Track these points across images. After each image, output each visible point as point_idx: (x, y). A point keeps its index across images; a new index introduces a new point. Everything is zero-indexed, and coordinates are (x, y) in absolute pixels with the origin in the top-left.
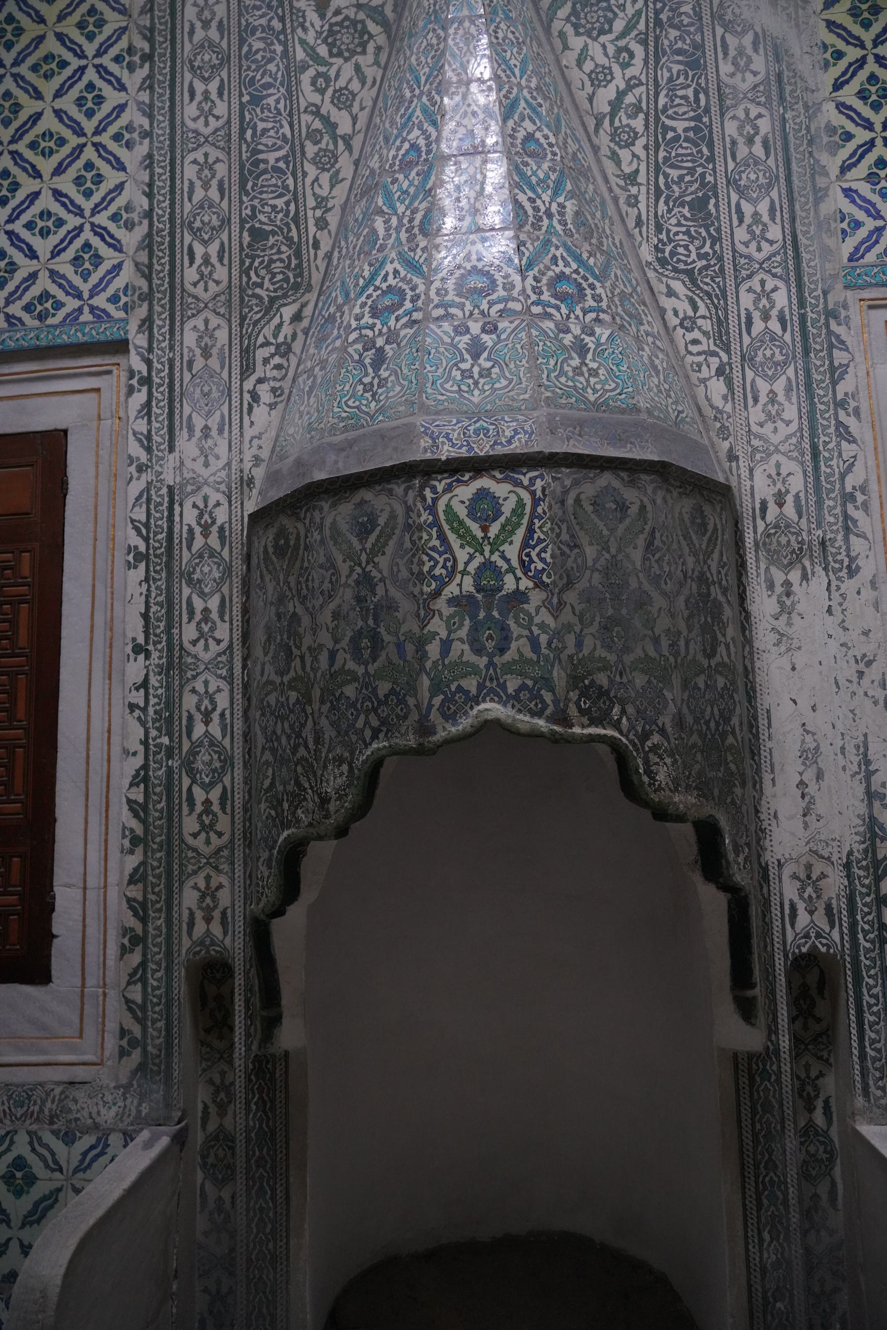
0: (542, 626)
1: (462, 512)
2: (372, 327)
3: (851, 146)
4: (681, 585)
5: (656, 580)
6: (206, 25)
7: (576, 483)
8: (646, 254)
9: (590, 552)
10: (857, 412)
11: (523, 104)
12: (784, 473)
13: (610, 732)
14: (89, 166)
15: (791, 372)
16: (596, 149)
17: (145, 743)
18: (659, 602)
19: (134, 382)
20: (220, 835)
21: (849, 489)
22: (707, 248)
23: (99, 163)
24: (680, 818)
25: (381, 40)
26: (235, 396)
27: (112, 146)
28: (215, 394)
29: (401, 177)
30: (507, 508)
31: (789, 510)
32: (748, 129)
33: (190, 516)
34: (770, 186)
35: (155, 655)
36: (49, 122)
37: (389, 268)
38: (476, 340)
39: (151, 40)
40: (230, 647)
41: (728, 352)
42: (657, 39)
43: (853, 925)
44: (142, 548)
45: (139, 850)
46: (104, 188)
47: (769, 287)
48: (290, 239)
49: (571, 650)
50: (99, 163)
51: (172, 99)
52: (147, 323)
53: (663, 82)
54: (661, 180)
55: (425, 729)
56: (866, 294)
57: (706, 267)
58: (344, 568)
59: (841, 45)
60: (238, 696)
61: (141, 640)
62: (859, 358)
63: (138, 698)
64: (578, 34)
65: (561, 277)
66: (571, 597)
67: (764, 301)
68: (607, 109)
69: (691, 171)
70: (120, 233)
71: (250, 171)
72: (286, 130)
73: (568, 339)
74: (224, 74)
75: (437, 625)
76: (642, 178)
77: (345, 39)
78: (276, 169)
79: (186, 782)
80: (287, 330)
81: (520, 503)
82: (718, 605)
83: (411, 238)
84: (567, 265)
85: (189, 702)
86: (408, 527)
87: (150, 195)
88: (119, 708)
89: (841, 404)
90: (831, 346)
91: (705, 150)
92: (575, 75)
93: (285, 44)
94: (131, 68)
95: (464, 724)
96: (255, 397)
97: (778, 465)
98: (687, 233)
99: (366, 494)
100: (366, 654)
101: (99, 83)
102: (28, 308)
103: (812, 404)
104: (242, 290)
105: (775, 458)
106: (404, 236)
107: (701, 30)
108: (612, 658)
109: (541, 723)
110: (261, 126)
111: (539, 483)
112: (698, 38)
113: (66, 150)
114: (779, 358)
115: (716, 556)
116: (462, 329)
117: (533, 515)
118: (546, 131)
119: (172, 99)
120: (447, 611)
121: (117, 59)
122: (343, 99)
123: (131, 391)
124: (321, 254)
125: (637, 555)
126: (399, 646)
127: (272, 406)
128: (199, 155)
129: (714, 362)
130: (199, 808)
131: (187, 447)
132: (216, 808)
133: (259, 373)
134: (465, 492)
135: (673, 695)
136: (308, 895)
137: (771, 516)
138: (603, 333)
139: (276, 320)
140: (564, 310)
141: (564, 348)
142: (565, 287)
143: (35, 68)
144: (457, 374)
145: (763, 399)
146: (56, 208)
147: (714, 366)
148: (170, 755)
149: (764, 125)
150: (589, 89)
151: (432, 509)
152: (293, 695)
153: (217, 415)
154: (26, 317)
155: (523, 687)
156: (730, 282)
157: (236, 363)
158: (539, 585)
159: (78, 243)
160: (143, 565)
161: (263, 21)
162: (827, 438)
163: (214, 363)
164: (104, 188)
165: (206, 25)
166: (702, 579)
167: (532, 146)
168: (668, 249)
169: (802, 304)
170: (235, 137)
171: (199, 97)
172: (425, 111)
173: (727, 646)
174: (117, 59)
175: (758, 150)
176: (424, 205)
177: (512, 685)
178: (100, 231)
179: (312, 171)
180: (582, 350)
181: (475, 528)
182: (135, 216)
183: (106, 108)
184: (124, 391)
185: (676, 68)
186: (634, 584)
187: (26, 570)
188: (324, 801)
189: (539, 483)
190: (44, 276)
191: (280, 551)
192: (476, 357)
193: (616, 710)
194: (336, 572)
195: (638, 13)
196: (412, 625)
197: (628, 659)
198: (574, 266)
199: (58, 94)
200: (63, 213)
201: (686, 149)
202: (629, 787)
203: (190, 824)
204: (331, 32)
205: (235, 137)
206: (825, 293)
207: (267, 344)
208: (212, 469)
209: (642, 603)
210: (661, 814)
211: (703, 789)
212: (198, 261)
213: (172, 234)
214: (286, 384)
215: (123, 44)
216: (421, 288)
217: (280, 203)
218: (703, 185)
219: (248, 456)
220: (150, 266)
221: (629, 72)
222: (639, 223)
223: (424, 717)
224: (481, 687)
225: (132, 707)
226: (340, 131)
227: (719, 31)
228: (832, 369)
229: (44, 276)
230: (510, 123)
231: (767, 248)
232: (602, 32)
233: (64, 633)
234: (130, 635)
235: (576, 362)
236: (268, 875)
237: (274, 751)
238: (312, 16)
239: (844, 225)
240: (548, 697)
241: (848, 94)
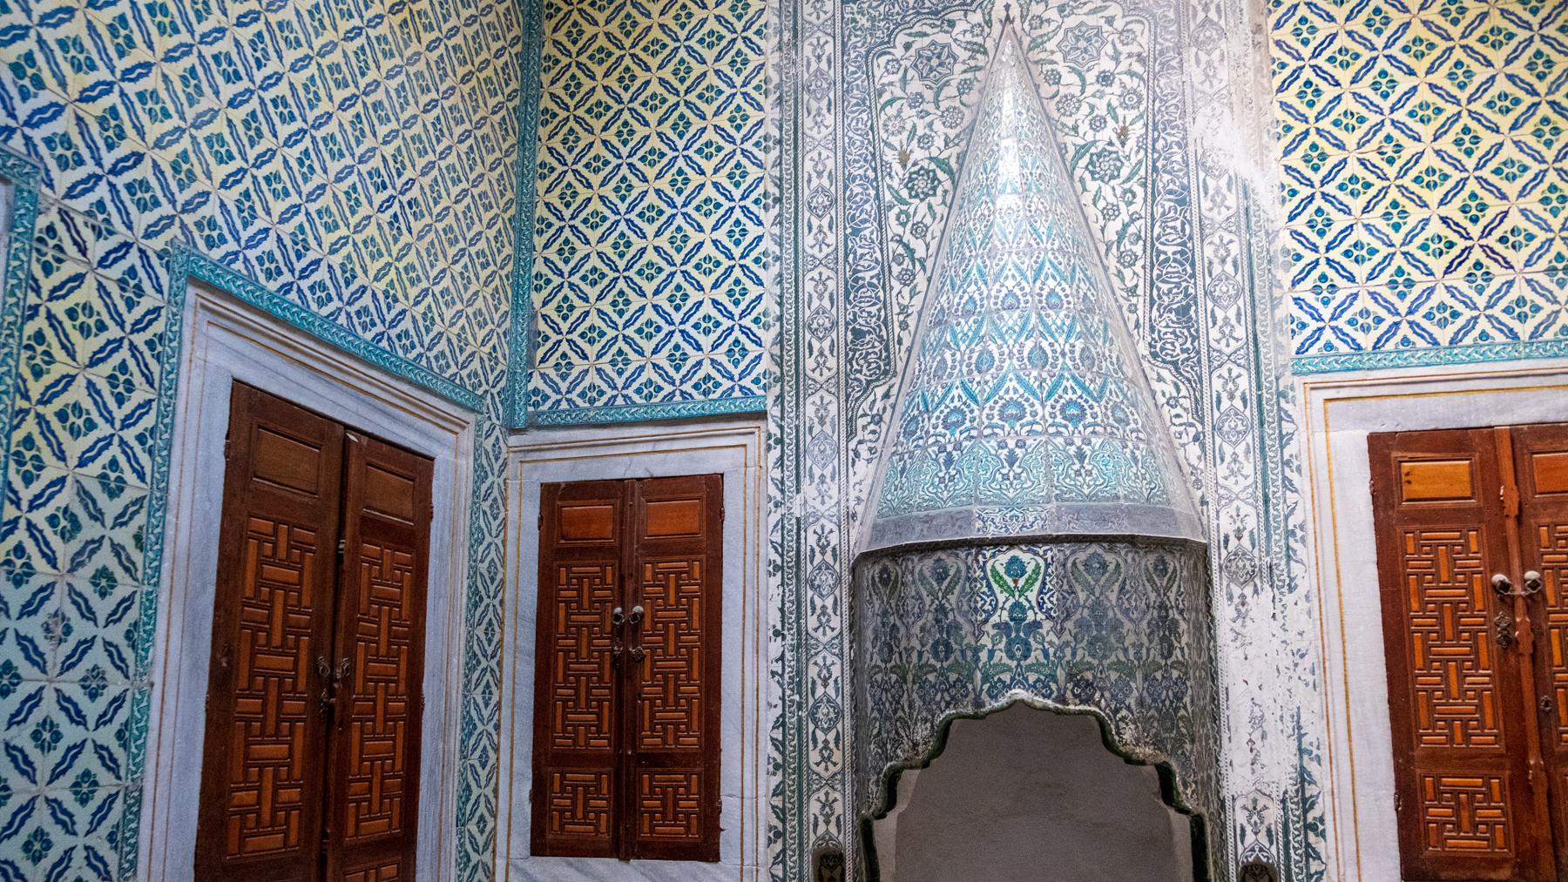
0: (1051, 643)
1: (1001, 571)
2: (944, 436)
3: (1301, 265)
4: (1145, 613)
5: (1126, 612)
6: (820, 174)
7: (1073, 552)
8: (1143, 349)
9: (1082, 596)
10: (1299, 469)
11: (1048, 265)
12: (1242, 514)
13: (1093, 708)
14: (737, 282)
15: (1249, 439)
16: (1106, 269)
17: (783, 699)
18: (1128, 625)
19: (771, 442)
20: (835, 764)
21: (1291, 527)
22: (1188, 345)
23: (744, 280)
24: (1143, 763)
25: (948, 185)
26: (843, 453)
27: (754, 267)
28: (829, 452)
29: (963, 321)
30: (1029, 569)
31: (1246, 542)
32: (1222, 252)
33: (812, 540)
34: (1237, 296)
35: (789, 637)
36: (709, 249)
37: (955, 392)
38: (1012, 452)
39: (780, 187)
40: (841, 633)
41: (1202, 423)
42: (1154, 182)
43: (1286, 844)
44: (779, 562)
45: (780, 773)
46: (748, 298)
47: (1234, 374)
48: (881, 337)
49: (1068, 657)
50: (744, 280)
51: (796, 232)
52: (780, 398)
53: (1157, 216)
54: (1155, 292)
55: (978, 704)
56: (1309, 379)
57: (1187, 359)
58: (928, 601)
59: (1296, 185)
60: (847, 668)
61: (779, 627)
62: (1302, 428)
63: (778, 667)
64: (1094, 179)
65: (1070, 402)
66: (1069, 625)
67: (1231, 385)
68: (1115, 237)
69: (1178, 285)
70: (760, 332)
71: (852, 286)
72: (878, 255)
73: (1072, 450)
74: (833, 212)
75: (986, 641)
76: (1140, 291)
77: (921, 184)
78: (870, 284)
79: (811, 727)
80: (879, 405)
81: (1038, 566)
82: (1175, 623)
83: (970, 372)
84: (1074, 392)
85: (813, 671)
86: (968, 579)
87: (781, 304)
88: (764, 674)
89: (1287, 463)
90: (1281, 419)
91: (1189, 270)
92: (1092, 212)
93: (877, 189)
94: (766, 208)
95: (1003, 701)
96: (857, 454)
97: (1238, 509)
98: (1174, 333)
99: (943, 555)
100: (942, 655)
101: (744, 220)
102: (696, 387)
103: (1265, 463)
104: (847, 375)
105: (1236, 503)
106: (965, 369)
107: (1187, 174)
108: (1096, 662)
109: (1050, 703)
110: (860, 251)
111: (1049, 554)
112: (1185, 181)
113: (721, 270)
114: (1240, 428)
115: (1175, 589)
116: (1002, 445)
117: (1046, 574)
118: (1064, 285)
119: (796, 232)
120: (993, 632)
121: (756, 202)
122: (920, 230)
123: (769, 448)
124: (903, 348)
125: (1113, 597)
126: (963, 652)
127: (869, 461)
128: (815, 274)
129: (1192, 431)
130: (820, 745)
131: (809, 489)
132: (832, 745)
133: (860, 436)
134: (1004, 558)
135: (1137, 685)
136: (901, 806)
137: (1231, 547)
138: (1097, 442)
139: (872, 398)
140: (1071, 428)
141: (1069, 457)
142: (1073, 411)
143: (698, 209)
144: (999, 477)
145: (1228, 459)
146: (714, 313)
147: (1191, 435)
148: (800, 708)
149: (1234, 249)
150: (1102, 222)
151: (983, 569)
152: (894, 677)
153: (830, 467)
154: (694, 393)
155: (1039, 680)
156: (1205, 370)
157: (843, 429)
158: (1049, 617)
159: (731, 339)
160: (779, 574)
161: (861, 172)
162: (1275, 489)
163: (828, 429)
164: (748, 298)
165: (820, 174)
166: (1162, 607)
167: (1054, 300)
168: (1159, 345)
169: (1259, 388)
170: (841, 259)
171: (815, 230)
172: (979, 271)
173: (1182, 649)
174: (756, 202)
175: (1229, 268)
176: (978, 348)
177: (1032, 678)
178: (745, 331)
179: (897, 285)
180: (1081, 456)
181: (1010, 581)
182: (770, 320)
183: (749, 239)
184: (763, 446)
185: (1168, 205)
186: (1111, 614)
187: (697, 574)
188: (915, 745)
189: (1049, 554)
190: (706, 363)
191: (885, 582)
192: (1011, 465)
193: (1097, 695)
194: (922, 602)
195: (1140, 162)
196: (970, 640)
197: (1106, 662)
198: (1079, 392)
199: (714, 229)
200: (719, 317)
201: (1174, 268)
202: (1109, 744)
203: (814, 756)
204: (911, 179)
205: (841, 259)
206: (1277, 379)
207: (865, 415)
208: (827, 506)
209: (1116, 626)
210: (1129, 760)
211: (1158, 743)
212: (816, 353)
213: (797, 333)
214: (879, 445)
215: (761, 190)
216: (976, 413)
217: (874, 310)
218: (1187, 296)
219: (853, 494)
220: (781, 357)
221: (1132, 209)
222: (1137, 326)
223: (978, 696)
224: (1012, 679)
225: (773, 674)
226: (917, 256)
227: (1202, 175)
228: (1281, 437)
229: (706, 363)
230: (1038, 283)
231: (1234, 345)
232: (1112, 177)
233: (724, 619)
234: (772, 623)
235: (1077, 467)
236: (875, 790)
237: (880, 711)
238: (897, 167)
239: (1294, 326)
240: (1054, 687)
241: (1300, 224)
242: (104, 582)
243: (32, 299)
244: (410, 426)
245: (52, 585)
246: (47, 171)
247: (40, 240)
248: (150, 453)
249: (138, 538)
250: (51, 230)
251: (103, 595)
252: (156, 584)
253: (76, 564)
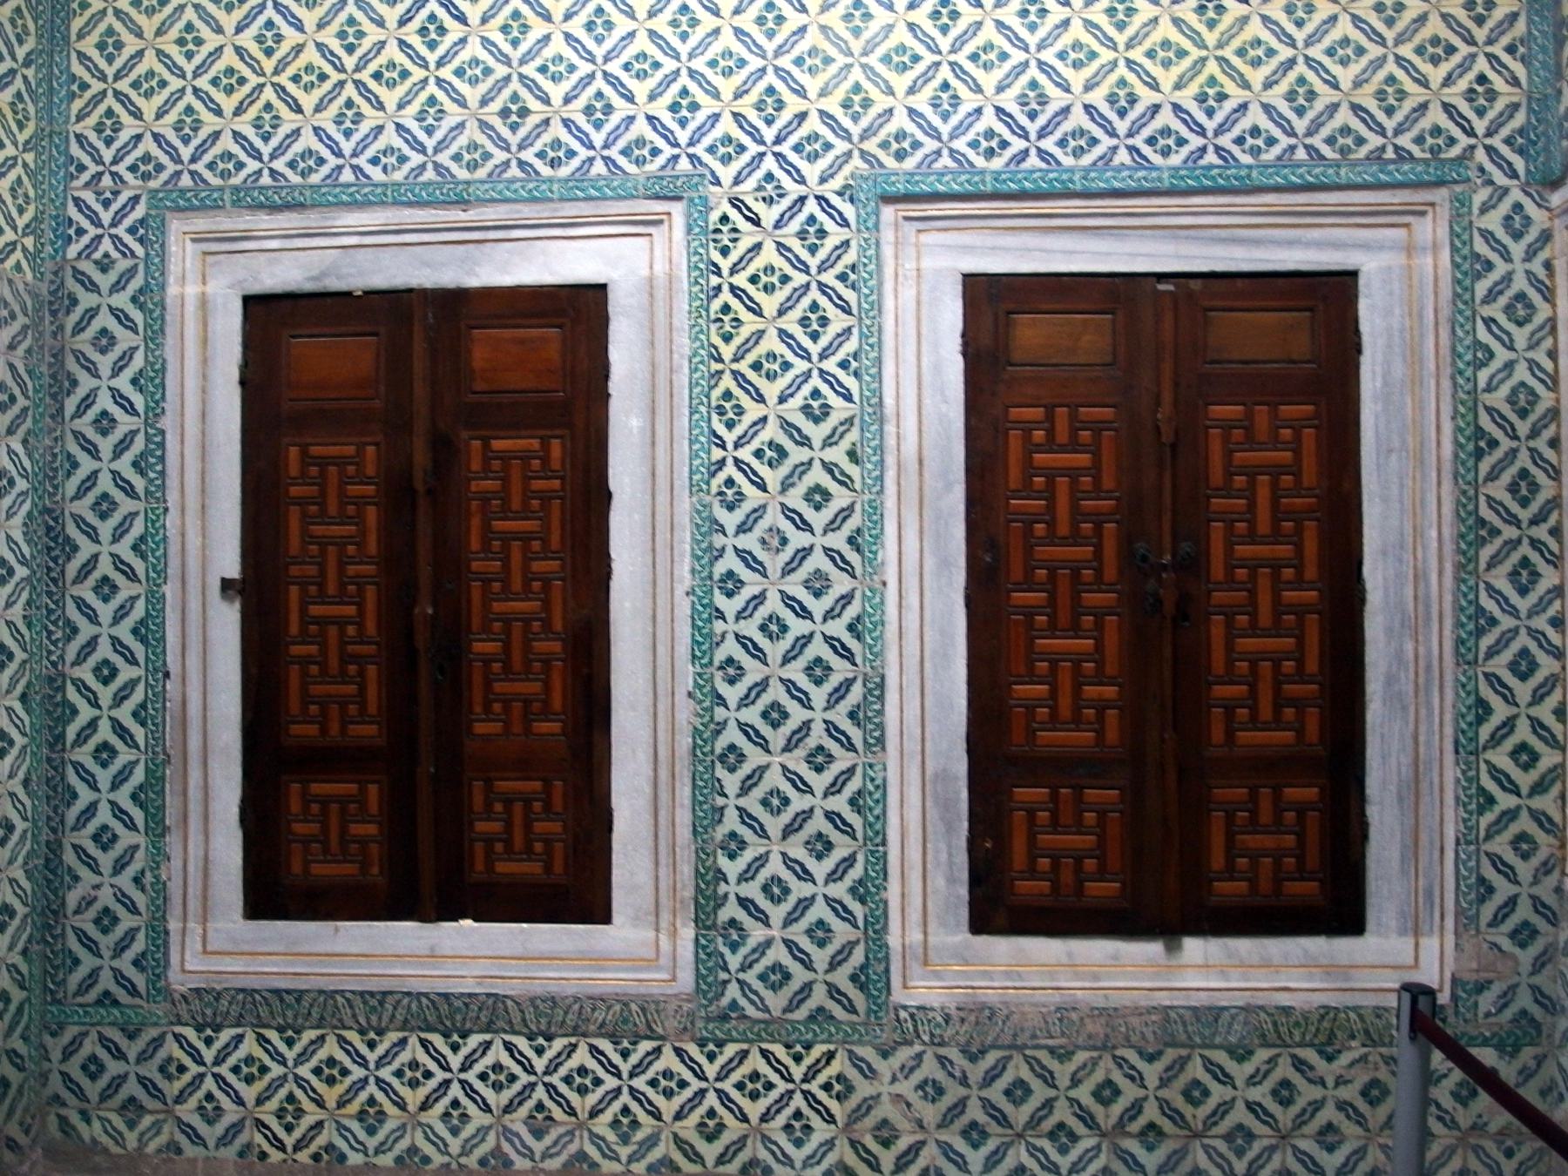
242: (818, 498)
243: (715, 280)
244: (1290, 243)
245: (764, 507)
246: (713, 173)
247: (717, 231)
248: (856, 374)
249: (852, 455)
250: (725, 219)
251: (818, 508)
252: (880, 492)
253: (786, 486)
